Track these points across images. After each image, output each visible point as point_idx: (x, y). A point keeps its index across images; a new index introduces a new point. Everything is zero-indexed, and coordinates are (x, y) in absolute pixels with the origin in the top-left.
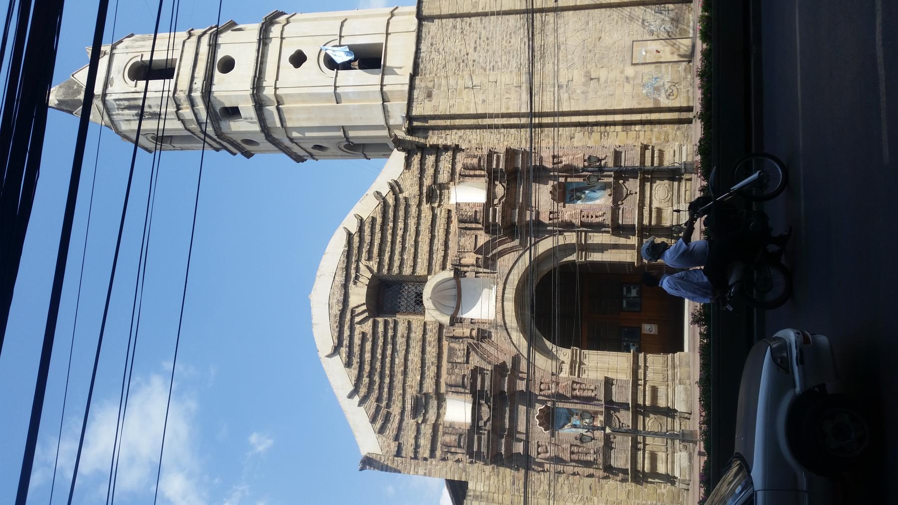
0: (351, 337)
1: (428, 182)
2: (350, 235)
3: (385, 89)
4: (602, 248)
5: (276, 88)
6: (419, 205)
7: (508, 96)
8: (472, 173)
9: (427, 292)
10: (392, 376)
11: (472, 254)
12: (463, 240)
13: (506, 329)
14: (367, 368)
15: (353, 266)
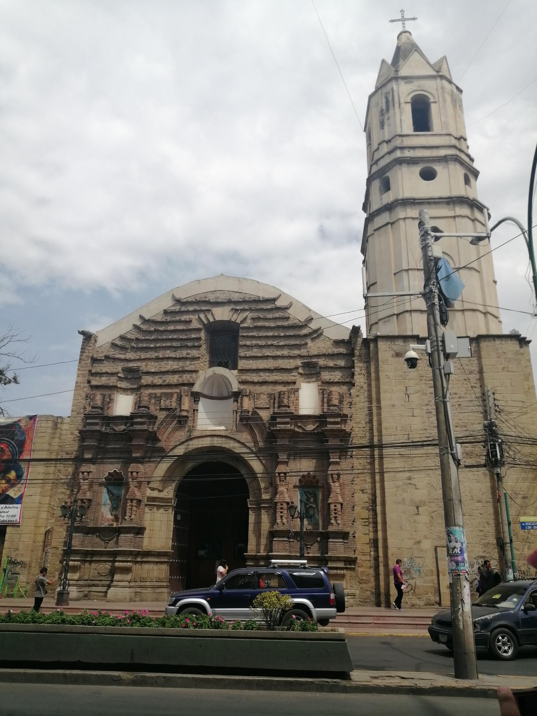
0: (188, 312)
1: (322, 362)
2: (274, 300)
3: (407, 315)
4: (258, 523)
5: (405, 219)
6: (300, 356)
7: (399, 428)
8: (325, 400)
9: (221, 371)
10: (155, 349)
11: (253, 406)
12: (265, 397)
13: (187, 441)
14: (162, 328)
15: (246, 307)
